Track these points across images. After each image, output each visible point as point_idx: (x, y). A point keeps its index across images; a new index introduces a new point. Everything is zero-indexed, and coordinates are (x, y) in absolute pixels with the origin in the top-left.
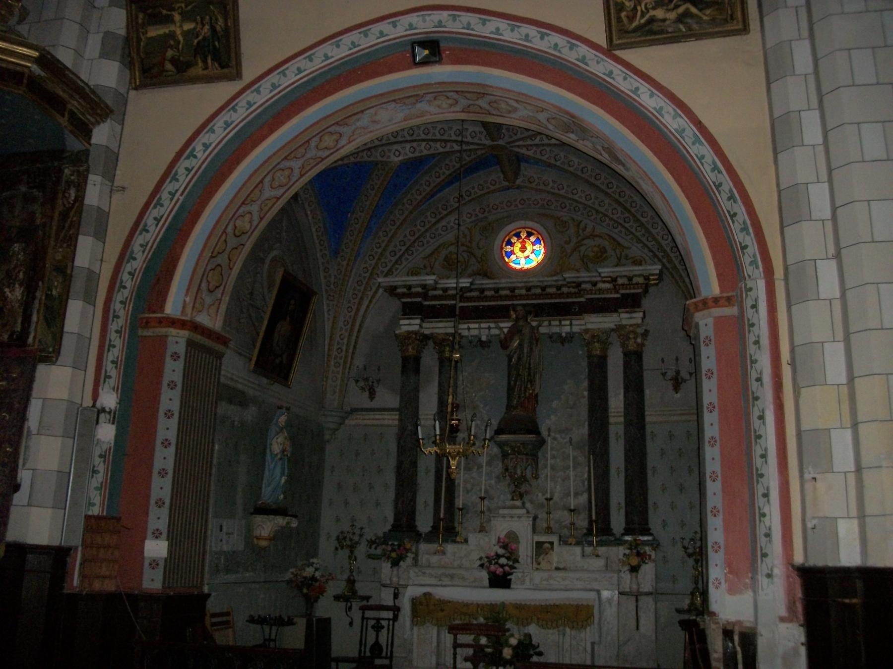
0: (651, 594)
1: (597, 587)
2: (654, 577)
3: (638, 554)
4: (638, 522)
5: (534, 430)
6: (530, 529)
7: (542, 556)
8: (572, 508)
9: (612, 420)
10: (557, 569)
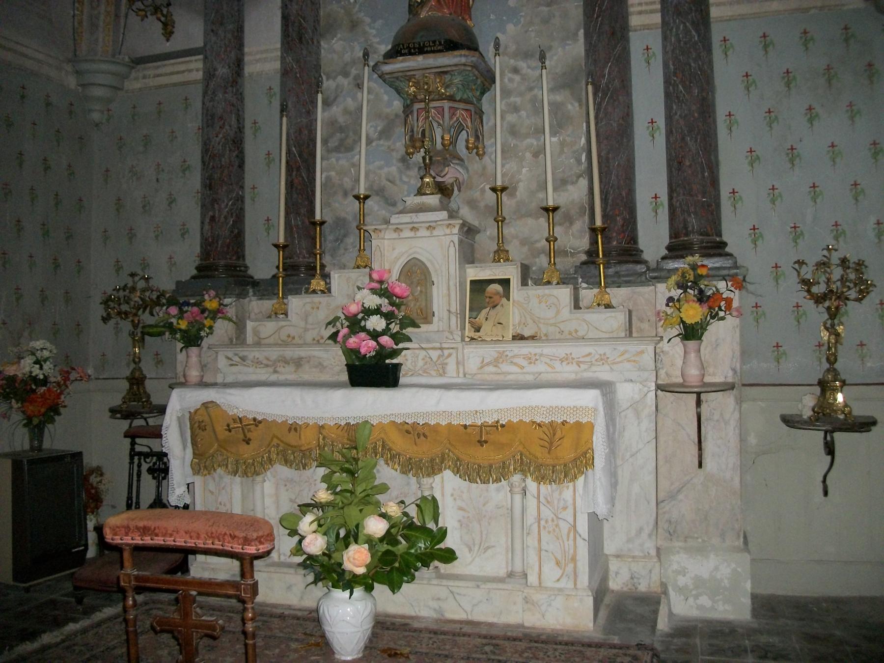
0: (730, 387)
1: (603, 374)
2: (737, 348)
3: (702, 298)
4: (698, 233)
5: (466, 42)
6: (453, 253)
7: (484, 312)
8: (551, 203)
9: (635, 21)
10: (519, 338)
